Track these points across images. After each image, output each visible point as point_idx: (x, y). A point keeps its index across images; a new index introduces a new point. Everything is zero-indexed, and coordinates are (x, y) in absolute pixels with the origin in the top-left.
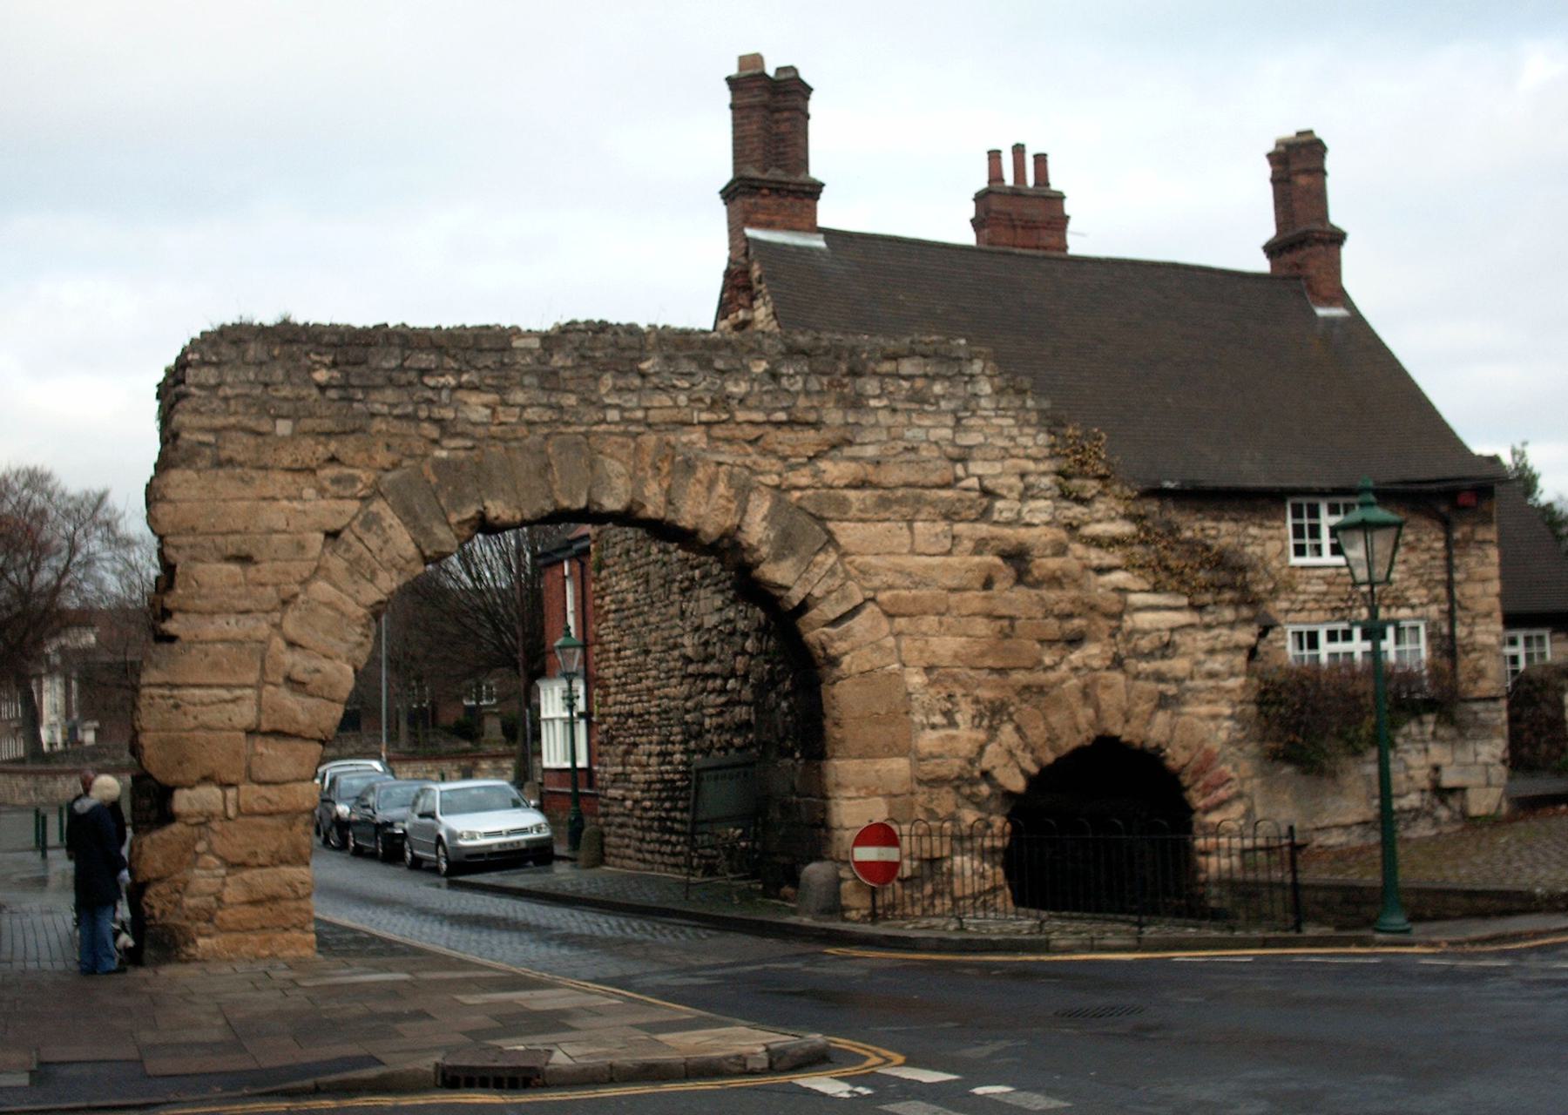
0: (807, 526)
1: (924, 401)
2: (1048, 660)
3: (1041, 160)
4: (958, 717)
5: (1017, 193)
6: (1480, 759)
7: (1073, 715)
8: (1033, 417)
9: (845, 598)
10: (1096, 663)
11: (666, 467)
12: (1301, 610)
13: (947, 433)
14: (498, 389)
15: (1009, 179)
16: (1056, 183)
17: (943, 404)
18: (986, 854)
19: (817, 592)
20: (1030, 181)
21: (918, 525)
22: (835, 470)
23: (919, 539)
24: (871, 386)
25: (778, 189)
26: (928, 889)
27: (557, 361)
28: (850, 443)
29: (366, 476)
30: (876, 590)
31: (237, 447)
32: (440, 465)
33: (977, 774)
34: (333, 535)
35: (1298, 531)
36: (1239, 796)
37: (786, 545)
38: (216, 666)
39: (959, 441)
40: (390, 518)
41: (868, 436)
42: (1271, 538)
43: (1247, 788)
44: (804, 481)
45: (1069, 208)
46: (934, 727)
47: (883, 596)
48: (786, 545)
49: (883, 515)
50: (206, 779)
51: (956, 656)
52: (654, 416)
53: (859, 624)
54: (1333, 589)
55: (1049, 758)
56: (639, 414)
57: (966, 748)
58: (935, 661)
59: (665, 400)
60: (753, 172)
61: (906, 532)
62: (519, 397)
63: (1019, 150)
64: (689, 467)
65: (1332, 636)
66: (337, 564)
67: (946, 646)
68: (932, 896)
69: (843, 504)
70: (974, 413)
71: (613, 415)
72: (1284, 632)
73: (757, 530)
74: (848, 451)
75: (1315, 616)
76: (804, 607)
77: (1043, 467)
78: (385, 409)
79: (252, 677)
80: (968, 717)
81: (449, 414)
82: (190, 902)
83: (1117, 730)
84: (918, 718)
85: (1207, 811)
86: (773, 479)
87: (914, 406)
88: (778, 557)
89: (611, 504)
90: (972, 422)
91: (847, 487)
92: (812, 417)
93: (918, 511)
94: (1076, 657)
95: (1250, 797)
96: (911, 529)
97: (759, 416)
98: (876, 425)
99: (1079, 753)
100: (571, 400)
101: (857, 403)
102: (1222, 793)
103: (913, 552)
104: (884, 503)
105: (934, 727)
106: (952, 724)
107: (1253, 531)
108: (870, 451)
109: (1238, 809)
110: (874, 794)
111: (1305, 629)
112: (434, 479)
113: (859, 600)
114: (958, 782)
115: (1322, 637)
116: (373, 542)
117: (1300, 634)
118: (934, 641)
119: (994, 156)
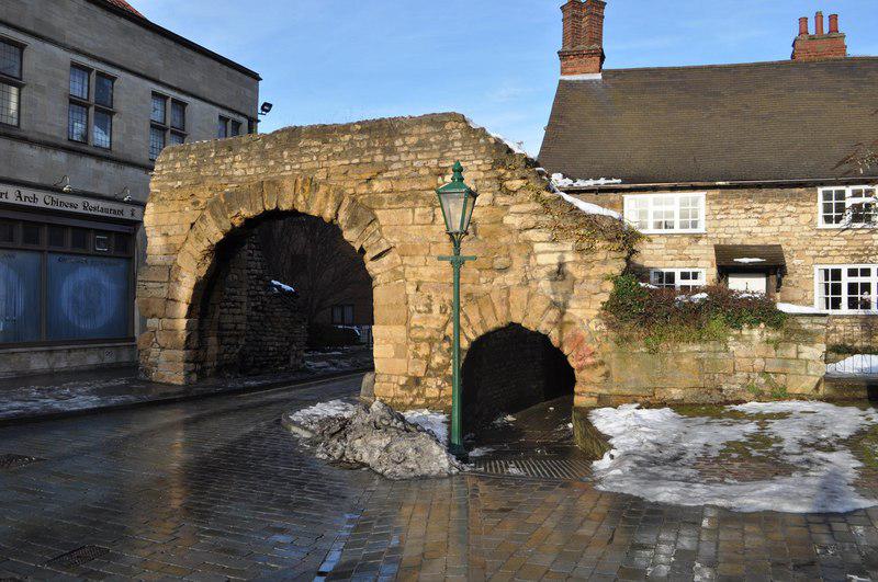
0: (364, 213)
1: (423, 146)
2: (482, 280)
3: (833, 18)
4: (433, 308)
5: (812, 38)
6: (802, 356)
7: (494, 310)
8: (483, 149)
9: (379, 246)
10: (509, 283)
11: (307, 188)
12: (825, 256)
13: (436, 161)
14: (246, 161)
15: (812, 31)
16: (841, 30)
17: (435, 147)
18: (448, 379)
19: (365, 245)
20: (826, 30)
21: (417, 211)
22: (377, 186)
23: (417, 218)
24: (398, 143)
25: (579, 54)
26: (415, 392)
27: (267, 146)
28: (386, 171)
29: (202, 201)
30: (395, 243)
31: (165, 195)
32: (225, 195)
33: (442, 336)
34: (192, 225)
35: (827, 208)
36: (602, 363)
37: (354, 221)
38: (156, 274)
39: (440, 165)
40: (209, 217)
41: (395, 166)
42: (804, 213)
43: (605, 360)
44: (364, 191)
45: (846, 42)
46: (419, 312)
47: (397, 246)
48: (354, 221)
49: (400, 205)
50: (153, 316)
51: (432, 276)
52: (305, 167)
53: (386, 259)
54: (851, 243)
55: (481, 332)
56: (297, 166)
57: (434, 325)
58: (422, 279)
59: (306, 159)
60: (568, 48)
61: (410, 213)
62: (254, 163)
63: (819, 16)
64: (317, 188)
65: (852, 273)
66: (192, 235)
67: (426, 273)
68: (418, 395)
69: (381, 200)
70: (450, 150)
71: (288, 167)
72: (812, 272)
73: (343, 217)
74: (385, 175)
75: (837, 260)
76: (362, 251)
77: (488, 175)
78: (210, 174)
79: (166, 279)
80: (438, 307)
81: (229, 173)
82: (150, 360)
83: (517, 318)
84: (412, 308)
85: (581, 369)
86: (351, 191)
87: (419, 149)
88: (349, 227)
89: (284, 207)
90: (448, 154)
91: (384, 192)
92: (369, 160)
93: (416, 202)
94: (499, 279)
95: (609, 365)
96: (414, 212)
97: (347, 162)
98: (400, 161)
99: (498, 330)
100: (272, 163)
101: (391, 151)
102: (589, 360)
103: (413, 224)
104: (400, 199)
105: (419, 312)
106: (430, 311)
107: (789, 208)
108: (396, 174)
109: (601, 370)
110: (388, 342)
111: (830, 267)
112: (223, 200)
113: (385, 247)
114: (431, 341)
115: (844, 274)
116: (203, 227)
117: (826, 271)
118: (422, 270)
119: (803, 21)
